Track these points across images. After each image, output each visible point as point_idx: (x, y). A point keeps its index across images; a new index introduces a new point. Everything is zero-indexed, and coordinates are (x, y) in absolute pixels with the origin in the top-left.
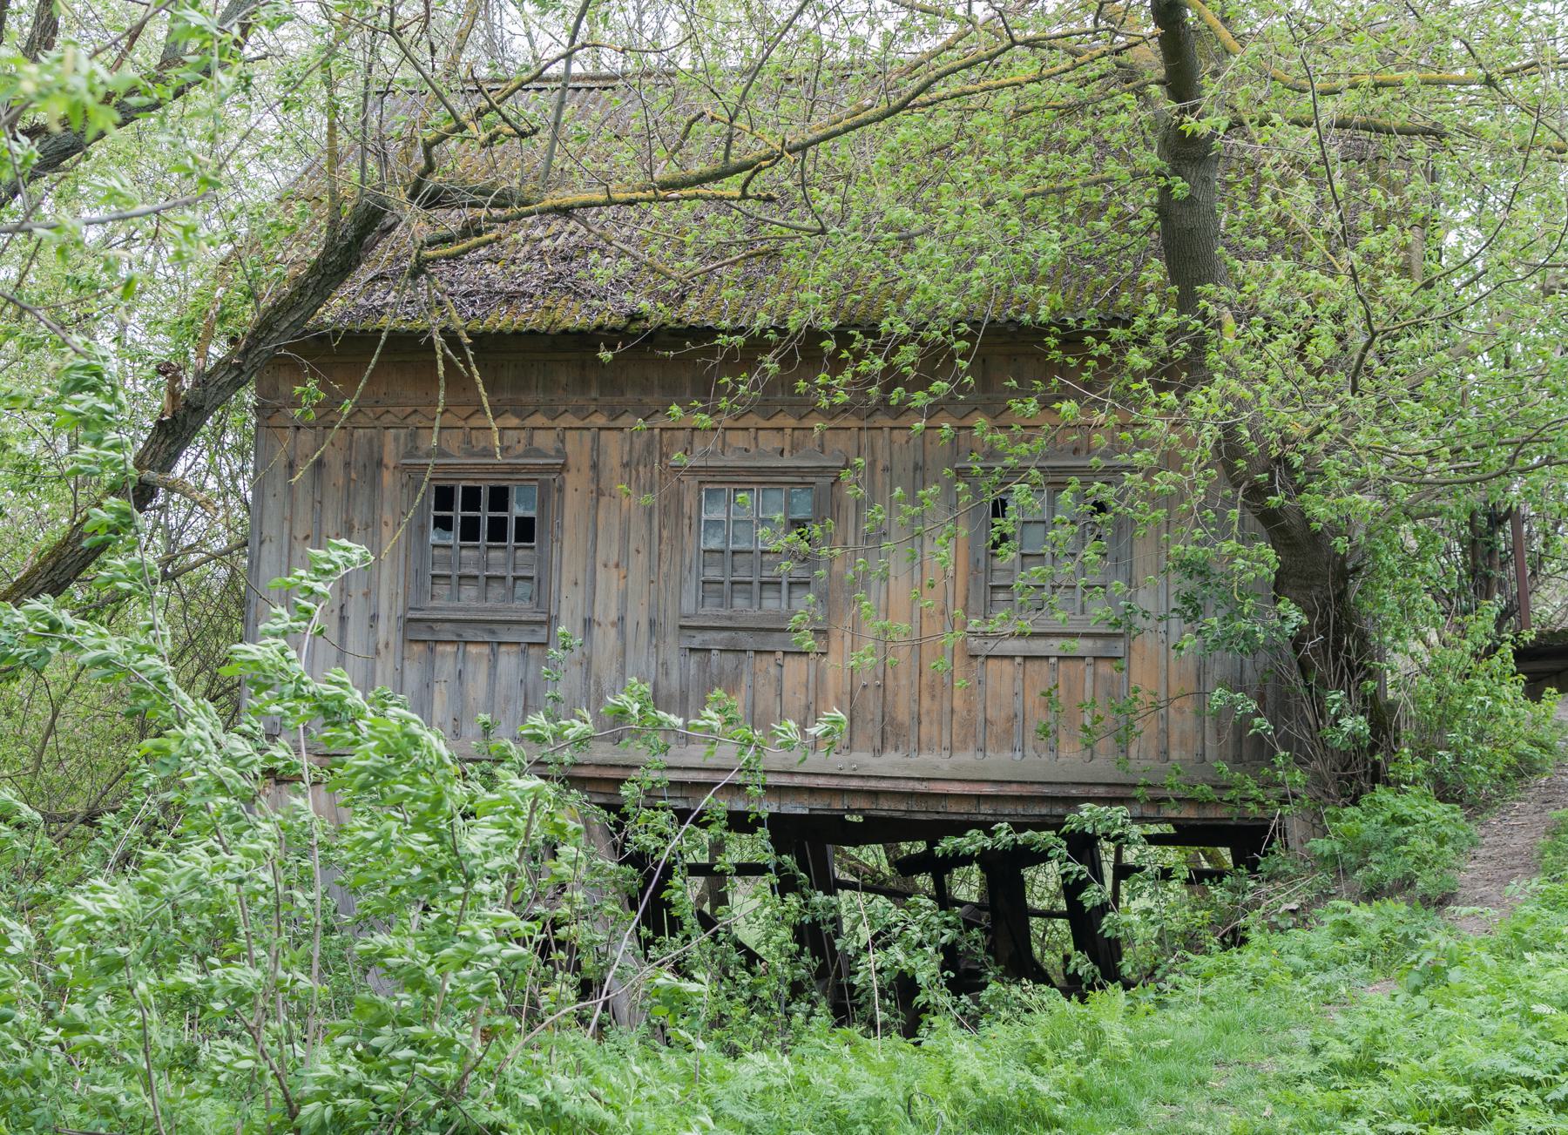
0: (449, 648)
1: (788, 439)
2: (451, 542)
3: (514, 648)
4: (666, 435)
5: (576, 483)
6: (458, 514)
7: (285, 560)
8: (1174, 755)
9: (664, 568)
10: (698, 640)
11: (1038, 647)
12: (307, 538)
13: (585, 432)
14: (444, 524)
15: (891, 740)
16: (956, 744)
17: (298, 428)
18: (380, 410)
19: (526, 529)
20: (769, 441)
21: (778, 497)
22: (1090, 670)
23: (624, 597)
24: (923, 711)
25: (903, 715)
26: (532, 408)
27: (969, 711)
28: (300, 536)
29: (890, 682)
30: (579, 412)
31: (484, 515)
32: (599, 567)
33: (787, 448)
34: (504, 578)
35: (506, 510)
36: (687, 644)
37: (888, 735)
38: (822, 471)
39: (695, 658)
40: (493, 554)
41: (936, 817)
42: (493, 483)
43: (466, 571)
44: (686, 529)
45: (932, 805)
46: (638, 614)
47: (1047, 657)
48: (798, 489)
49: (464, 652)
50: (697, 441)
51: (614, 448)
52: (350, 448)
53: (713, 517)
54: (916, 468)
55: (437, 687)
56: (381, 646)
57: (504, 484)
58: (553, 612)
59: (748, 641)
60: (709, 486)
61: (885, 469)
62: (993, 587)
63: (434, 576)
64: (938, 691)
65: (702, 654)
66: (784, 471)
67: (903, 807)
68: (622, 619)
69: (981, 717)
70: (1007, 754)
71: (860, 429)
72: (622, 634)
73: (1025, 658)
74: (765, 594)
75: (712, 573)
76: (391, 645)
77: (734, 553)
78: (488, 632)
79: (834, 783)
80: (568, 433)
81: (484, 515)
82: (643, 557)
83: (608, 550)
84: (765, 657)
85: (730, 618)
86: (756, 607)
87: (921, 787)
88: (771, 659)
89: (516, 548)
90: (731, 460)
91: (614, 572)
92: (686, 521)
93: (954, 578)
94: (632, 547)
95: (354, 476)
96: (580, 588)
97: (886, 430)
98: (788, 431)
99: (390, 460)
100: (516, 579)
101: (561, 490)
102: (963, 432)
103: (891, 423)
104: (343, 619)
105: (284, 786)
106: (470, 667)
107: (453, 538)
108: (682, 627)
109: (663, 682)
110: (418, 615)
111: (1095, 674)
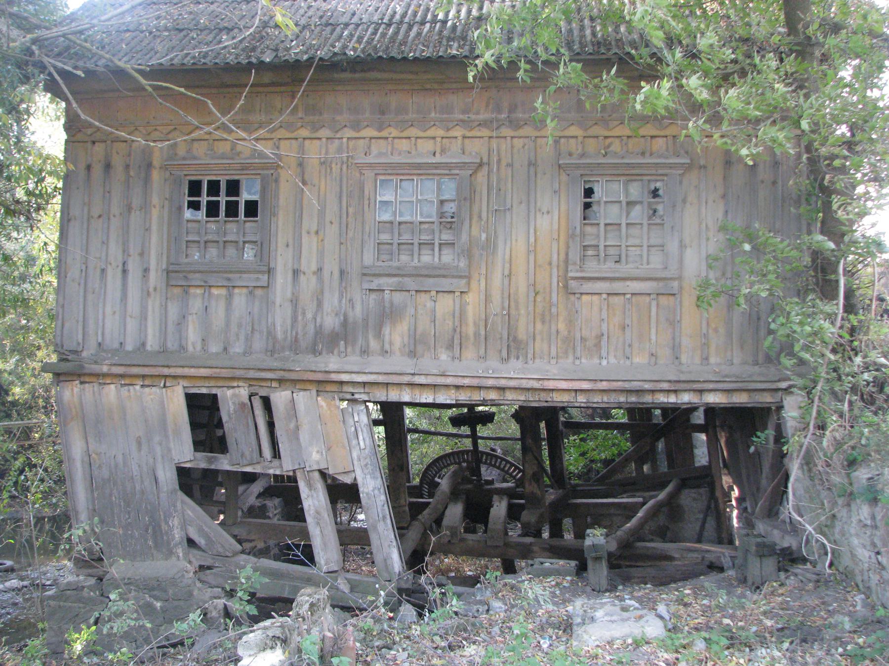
0: (199, 291)
1: (438, 144)
2: (200, 218)
3: (245, 291)
4: (351, 143)
5: (288, 176)
6: (204, 199)
7: (85, 232)
8: (712, 360)
9: (350, 234)
10: (376, 283)
11: (618, 287)
12: (100, 216)
13: (293, 141)
14: (194, 206)
15: (514, 352)
16: (560, 355)
17: (94, 143)
18: (150, 129)
19: (252, 209)
20: (426, 146)
21: (431, 185)
22: (654, 303)
23: (321, 253)
24: (537, 332)
25: (522, 334)
26: (256, 125)
27: (569, 332)
28: (96, 215)
29: (513, 312)
30: (290, 127)
31: (223, 199)
32: (304, 234)
33: (438, 151)
34: (236, 242)
35: (237, 195)
36: (366, 286)
37: (514, 347)
38: (463, 166)
39: (373, 296)
40: (229, 226)
41: (545, 404)
42: (228, 178)
43: (210, 237)
44: (366, 207)
45: (543, 396)
46: (331, 267)
47: (624, 294)
48: (445, 179)
49: (210, 293)
50: (373, 147)
51: (314, 152)
52: (130, 155)
53: (385, 199)
54: (530, 164)
55: (190, 318)
56: (151, 290)
57: (236, 178)
59: (410, 283)
60: (382, 177)
61: (508, 165)
62: (584, 246)
63: (187, 242)
64: (547, 318)
65: (378, 293)
66: (437, 166)
67: (523, 398)
68: (320, 270)
69: (578, 336)
70: (596, 361)
71: (490, 137)
72: (320, 280)
73: (608, 294)
74: (423, 252)
75: (385, 237)
76: (158, 289)
77: (400, 223)
78: (226, 276)
79: (475, 382)
80: (282, 143)
81: (223, 199)
82: (335, 228)
83: (310, 223)
84: (423, 294)
85: (399, 268)
86: (416, 261)
87: (536, 385)
88: (427, 296)
89: (245, 222)
90: (396, 159)
91: (315, 239)
92: (366, 202)
93: (558, 240)
94: (328, 219)
95: (132, 173)
96: (291, 248)
97: (509, 138)
98: (439, 140)
99: (156, 162)
100: (244, 242)
101: (277, 181)
102: (563, 140)
103: (513, 134)
104: (125, 271)
105: (87, 385)
106: (213, 303)
107: (201, 214)
108: (364, 275)
109: (350, 314)
110: (177, 268)
111: (658, 305)
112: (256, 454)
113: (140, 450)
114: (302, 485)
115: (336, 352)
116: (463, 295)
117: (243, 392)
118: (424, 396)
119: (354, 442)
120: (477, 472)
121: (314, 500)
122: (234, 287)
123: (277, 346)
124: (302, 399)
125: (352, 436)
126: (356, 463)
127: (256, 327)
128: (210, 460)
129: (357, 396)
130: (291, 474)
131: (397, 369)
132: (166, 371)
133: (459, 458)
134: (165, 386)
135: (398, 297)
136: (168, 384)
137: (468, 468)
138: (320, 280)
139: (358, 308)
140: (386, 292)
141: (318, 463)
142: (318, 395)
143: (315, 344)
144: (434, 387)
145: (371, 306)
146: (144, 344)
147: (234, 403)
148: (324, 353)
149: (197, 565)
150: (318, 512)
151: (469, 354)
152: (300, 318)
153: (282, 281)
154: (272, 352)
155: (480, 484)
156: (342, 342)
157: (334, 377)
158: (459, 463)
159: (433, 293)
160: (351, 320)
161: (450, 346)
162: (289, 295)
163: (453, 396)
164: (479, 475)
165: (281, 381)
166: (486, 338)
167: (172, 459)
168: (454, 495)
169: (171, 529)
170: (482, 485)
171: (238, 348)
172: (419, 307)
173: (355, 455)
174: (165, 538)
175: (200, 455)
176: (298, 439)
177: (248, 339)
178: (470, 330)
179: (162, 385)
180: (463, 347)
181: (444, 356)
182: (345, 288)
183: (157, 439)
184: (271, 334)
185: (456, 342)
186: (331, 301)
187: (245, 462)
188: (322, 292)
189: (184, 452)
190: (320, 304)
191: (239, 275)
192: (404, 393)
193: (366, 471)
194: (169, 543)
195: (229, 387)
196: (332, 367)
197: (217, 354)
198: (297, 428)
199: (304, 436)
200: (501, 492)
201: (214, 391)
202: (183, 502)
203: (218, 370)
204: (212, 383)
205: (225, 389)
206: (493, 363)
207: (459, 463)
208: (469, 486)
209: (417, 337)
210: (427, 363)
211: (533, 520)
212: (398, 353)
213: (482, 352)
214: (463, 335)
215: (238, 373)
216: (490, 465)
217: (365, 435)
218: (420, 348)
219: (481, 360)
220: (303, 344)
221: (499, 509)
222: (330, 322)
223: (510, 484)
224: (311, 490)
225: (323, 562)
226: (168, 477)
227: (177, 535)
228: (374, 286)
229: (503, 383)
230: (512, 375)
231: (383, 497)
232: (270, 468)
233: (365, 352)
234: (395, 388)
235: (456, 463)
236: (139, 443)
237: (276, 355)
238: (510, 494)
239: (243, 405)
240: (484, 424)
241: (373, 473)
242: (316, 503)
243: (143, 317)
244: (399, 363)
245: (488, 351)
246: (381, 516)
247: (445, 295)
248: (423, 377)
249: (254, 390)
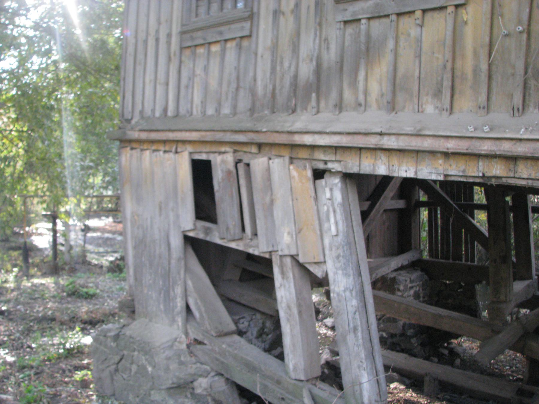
36: (340, 18)
39: (350, 30)
56: (172, 55)
58: (255, 10)
65: (354, 26)
72: (298, 19)
79: (462, 146)
109: (325, 56)
112: (238, 230)
113: (160, 215)
114: (276, 270)
115: (309, 108)
116: (462, 11)
117: (230, 158)
118: (404, 168)
119: (326, 226)
121: (286, 290)
122: (226, 41)
123: (258, 104)
124: (278, 165)
125: (323, 217)
126: (327, 252)
127: (241, 84)
128: (207, 231)
129: (330, 166)
130: (267, 256)
131: (362, 128)
132: (171, 136)
134: (176, 152)
135: (377, 26)
136: (179, 150)
138: (298, 19)
139: (333, 47)
140: (363, 21)
141: (288, 247)
142: (291, 163)
143: (289, 99)
144: (417, 154)
145: (347, 44)
146: (165, 110)
147: (222, 171)
148: (298, 110)
149: (192, 338)
150: (289, 307)
151: (465, 103)
152: (278, 68)
153: (265, 25)
154: (252, 110)
156: (314, 95)
157: (298, 139)
159: (418, 14)
160: (325, 65)
161: (438, 94)
162: (269, 43)
163: (441, 169)
165: (260, 146)
166: (490, 77)
167: (180, 227)
169: (175, 297)
171: (226, 110)
172: (402, 38)
173: (327, 241)
174: (171, 304)
175: (201, 224)
176: (272, 215)
177: (235, 98)
178: (467, 64)
179: (174, 150)
180: (457, 91)
181: (430, 109)
182: (320, 24)
183: (171, 204)
184: (253, 92)
185: (447, 84)
186: (308, 44)
187: (229, 237)
188: (298, 34)
189: (187, 220)
190: (295, 48)
191: (227, 27)
192: (379, 162)
193: (338, 265)
194: (173, 311)
195: (220, 153)
196: (298, 126)
197: (212, 116)
198: (272, 202)
199: (278, 213)
201: (211, 157)
202: (187, 269)
203: (203, 133)
204: (208, 148)
205: (217, 154)
206: (500, 116)
209: (398, 81)
210: (406, 120)
212: (374, 106)
213: (483, 98)
214: (458, 73)
215: (219, 136)
217: (339, 217)
218: (400, 98)
219: (482, 112)
220: (281, 99)
222: (306, 71)
224: (283, 278)
225: (291, 366)
226: (177, 242)
227: (180, 304)
228: (348, 17)
229: (506, 148)
230: (522, 134)
231: (354, 302)
232: (251, 247)
233: (340, 106)
234: (369, 154)
236: (160, 209)
237: (256, 115)
239: (229, 172)
241: (345, 269)
242: (288, 294)
243: (167, 84)
244: (374, 119)
245: (494, 98)
246: (351, 325)
247: (436, 14)
248: (393, 138)
249: (240, 155)
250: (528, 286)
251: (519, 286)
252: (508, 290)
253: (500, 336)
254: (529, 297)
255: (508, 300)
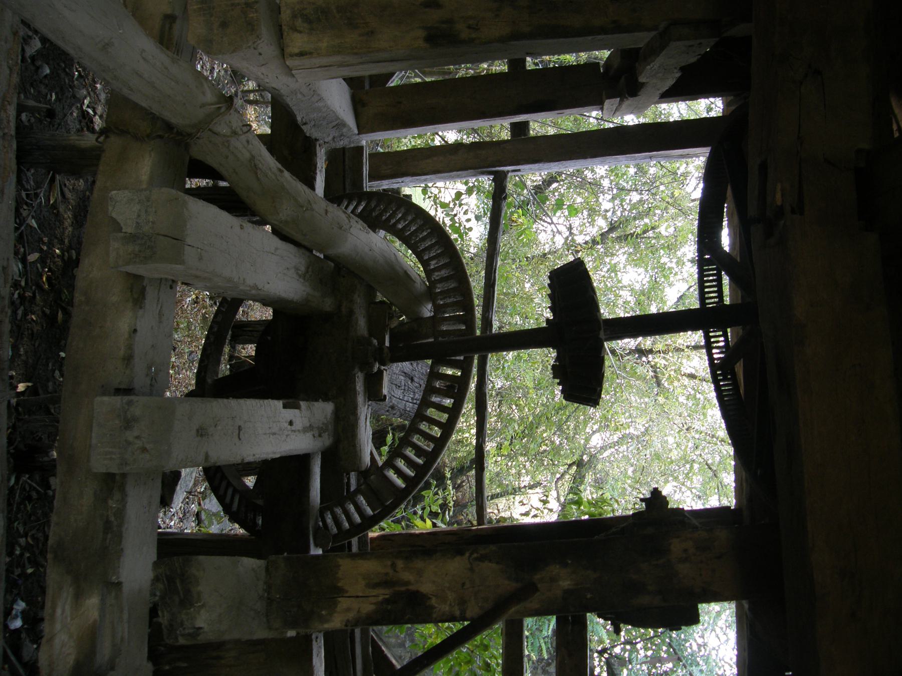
120: (406, 348)
133: (445, 293)
137: (418, 320)
155: (370, 361)
158: (430, 294)
164: (397, 356)
168: (338, 274)
170: (365, 366)
200: (344, 427)
207: (430, 294)
208: (362, 324)
211: (200, 623)
216: (430, 390)
221: (277, 430)
223: (367, 447)
235: (433, 284)
238: (339, 453)
240: (558, 371)
250: (341, 125)
251: (336, 97)
252: (325, 61)
253: (146, 44)
254: (307, 130)
255: (289, 62)
